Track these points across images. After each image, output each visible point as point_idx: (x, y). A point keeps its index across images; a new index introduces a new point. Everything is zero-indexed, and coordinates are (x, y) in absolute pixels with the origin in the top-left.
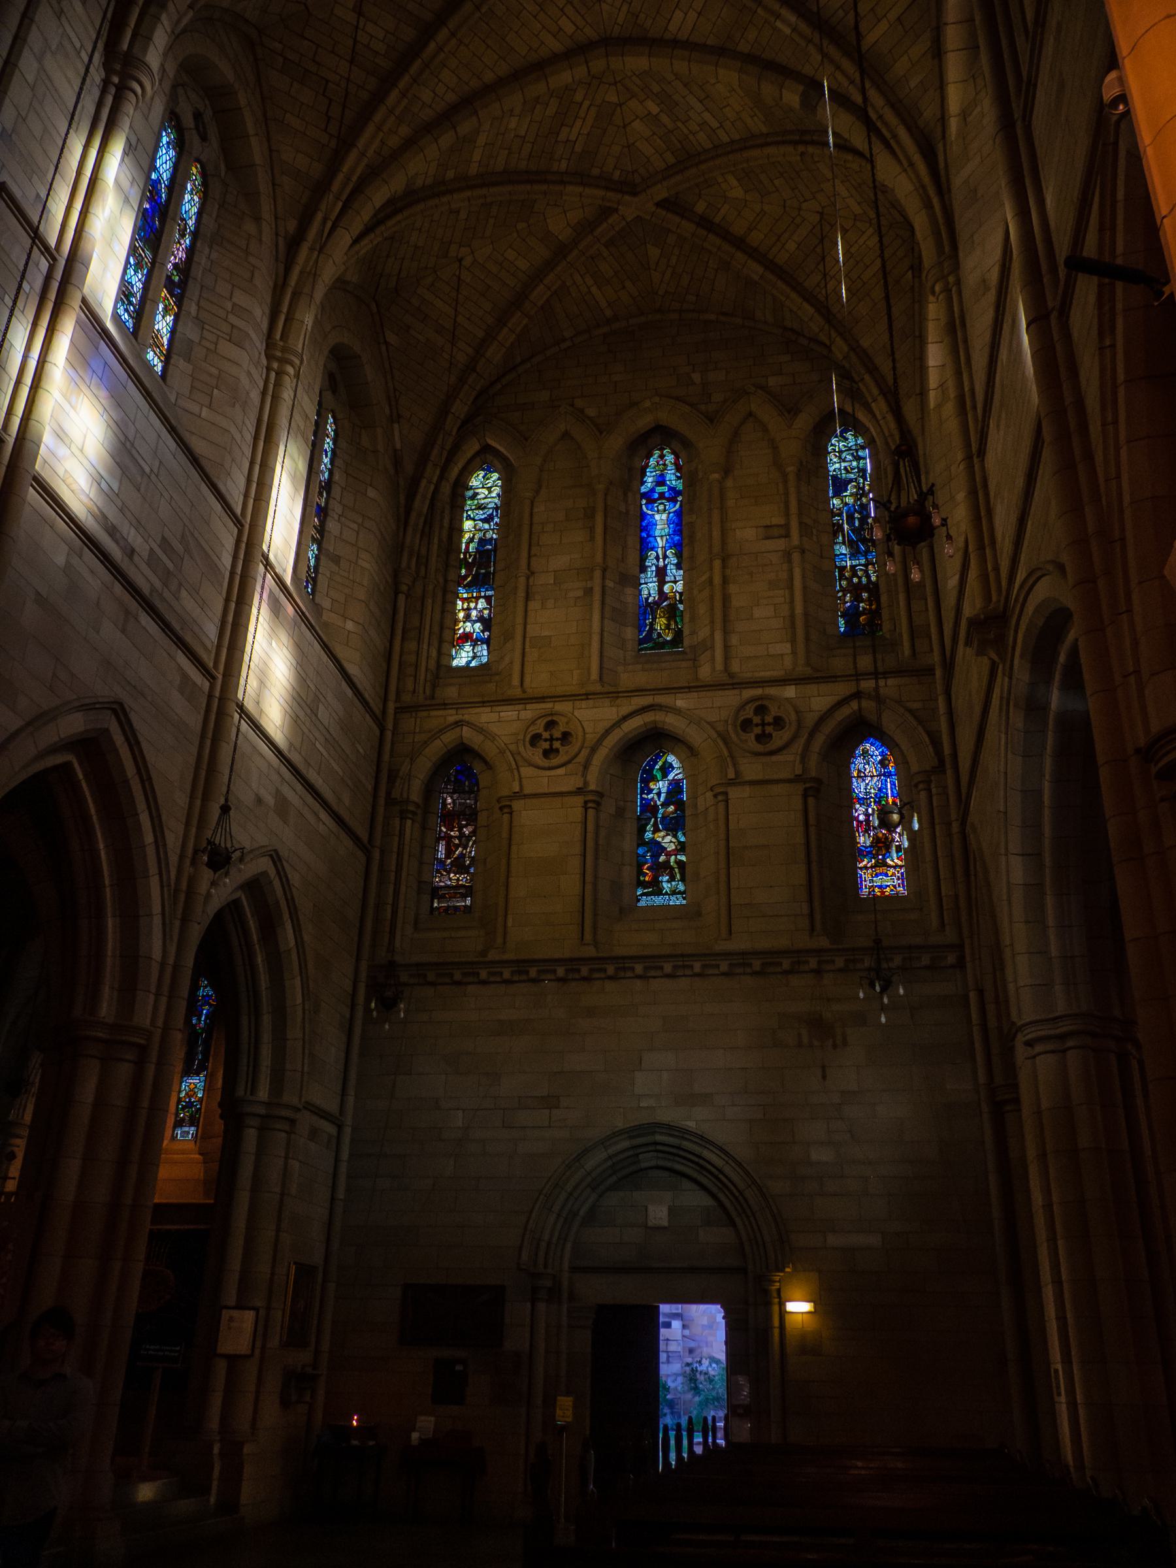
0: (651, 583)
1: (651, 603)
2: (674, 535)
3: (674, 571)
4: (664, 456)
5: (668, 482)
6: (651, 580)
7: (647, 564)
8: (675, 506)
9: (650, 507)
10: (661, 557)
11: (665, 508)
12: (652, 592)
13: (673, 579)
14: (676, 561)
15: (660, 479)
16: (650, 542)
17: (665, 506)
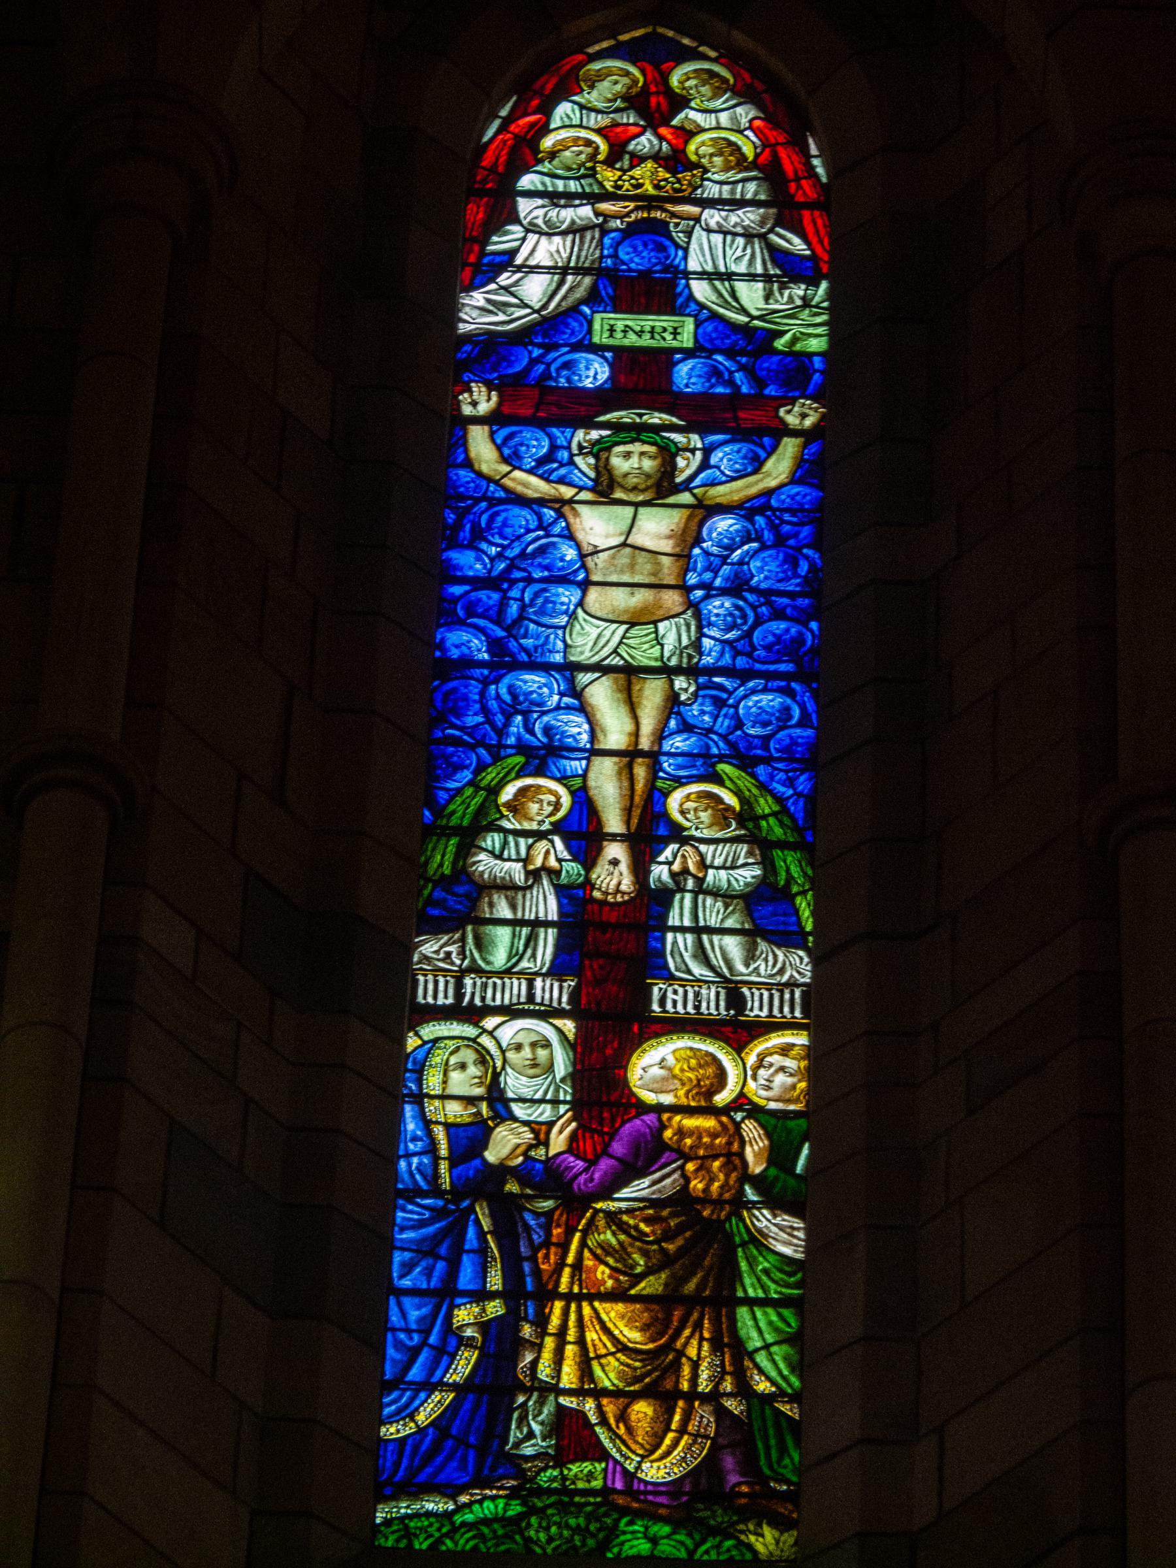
0: (511, 1012)
1: (502, 1171)
2: (743, 676)
3: (733, 945)
4: (681, 102)
5: (701, 290)
6: (516, 989)
7: (484, 864)
8: (756, 464)
9: (536, 444)
10: (614, 823)
11: (668, 467)
12: (515, 1084)
13: (713, 1003)
14: (747, 876)
15: (634, 259)
16: (519, 705)
17: (668, 455)
